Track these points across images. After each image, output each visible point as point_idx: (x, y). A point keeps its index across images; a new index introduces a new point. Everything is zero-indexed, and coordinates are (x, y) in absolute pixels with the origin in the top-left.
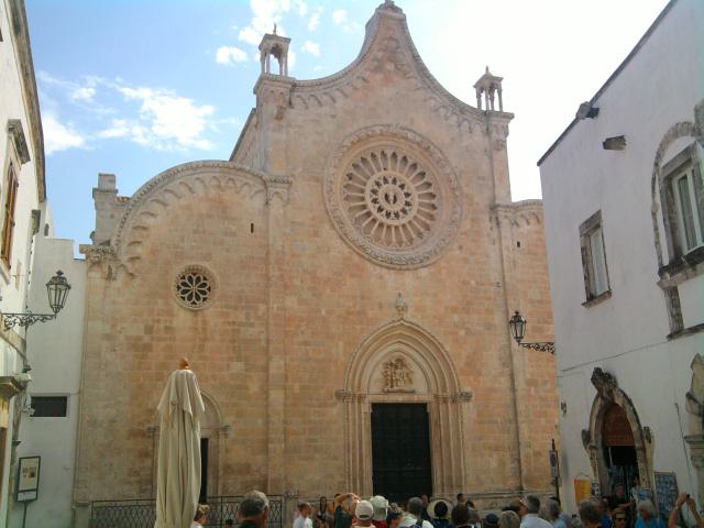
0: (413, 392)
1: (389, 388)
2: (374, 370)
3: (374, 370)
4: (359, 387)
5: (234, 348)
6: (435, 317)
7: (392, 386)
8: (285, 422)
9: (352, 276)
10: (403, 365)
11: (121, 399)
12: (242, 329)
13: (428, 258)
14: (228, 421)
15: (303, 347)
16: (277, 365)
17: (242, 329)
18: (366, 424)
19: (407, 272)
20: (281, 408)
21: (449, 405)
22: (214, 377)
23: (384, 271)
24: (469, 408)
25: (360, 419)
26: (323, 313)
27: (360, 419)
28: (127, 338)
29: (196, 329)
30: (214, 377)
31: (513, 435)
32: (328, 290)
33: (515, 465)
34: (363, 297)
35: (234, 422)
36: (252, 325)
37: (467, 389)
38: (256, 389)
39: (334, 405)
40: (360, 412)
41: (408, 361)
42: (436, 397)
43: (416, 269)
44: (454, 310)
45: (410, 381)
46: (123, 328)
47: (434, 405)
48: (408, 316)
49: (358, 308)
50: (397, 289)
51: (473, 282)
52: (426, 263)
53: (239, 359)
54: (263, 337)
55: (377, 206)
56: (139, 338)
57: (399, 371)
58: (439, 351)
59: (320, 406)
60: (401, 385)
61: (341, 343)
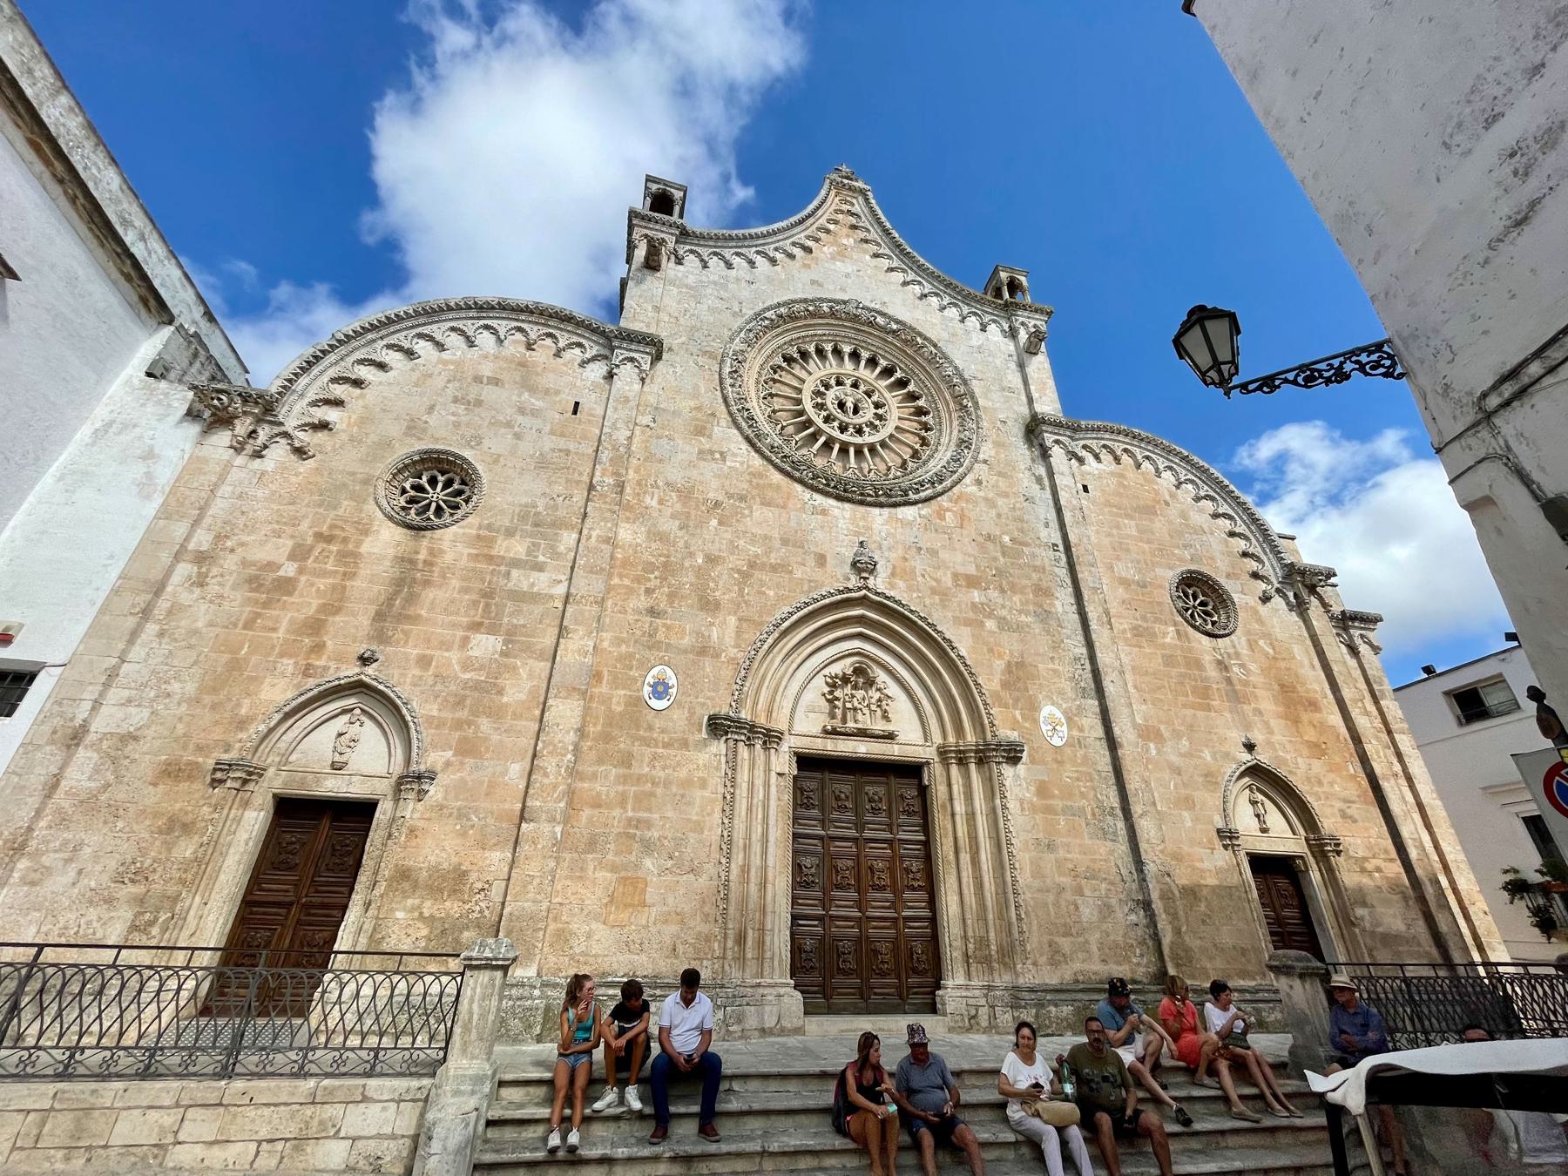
0: (890, 736)
1: (837, 723)
2: (803, 688)
3: (803, 688)
4: (770, 712)
5: (487, 605)
6: (934, 591)
7: (844, 720)
8: (573, 772)
9: (766, 503)
10: (870, 683)
11: (176, 686)
12: (515, 573)
13: (917, 491)
14: (432, 759)
15: (648, 619)
16: (574, 651)
17: (515, 573)
18: (780, 798)
19: (876, 511)
20: (572, 737)
21: (973, 767)
22: (425, 662)
23: (832, 502)
24: (1016, 777)
25: (767, 785)
26: (700, 561)
27: (767, 785)
28: (245, 563)
29: (412, 562)
30: (425, 662)
31: (1123, 847)
32: (714, 522)
33: (1138, 917)
34: (785, 542)
35: (448, 764)
36: (540, 568)
37: (1008, 734)
38: (523, 697)
39: (704, 743)
40: (768, 770)
41: (882, 677)
42: (943, 752)
43: (895, 505)
44: (972, 582)
45: (886, 717)
46: (242, 544)
47: (938, 769)
48: (879, 582)
49: (774, 559)
50: (857, 534)
51: (1006, 539)
52: (912, 496)
53: (493, 630)
54: (561, 590)
55: (824, 413)
56: (272, 566)
57: (860, 694)
58: (943, 654)
59: (666, 746)
60: (865, 721)
61: (732, 621)
